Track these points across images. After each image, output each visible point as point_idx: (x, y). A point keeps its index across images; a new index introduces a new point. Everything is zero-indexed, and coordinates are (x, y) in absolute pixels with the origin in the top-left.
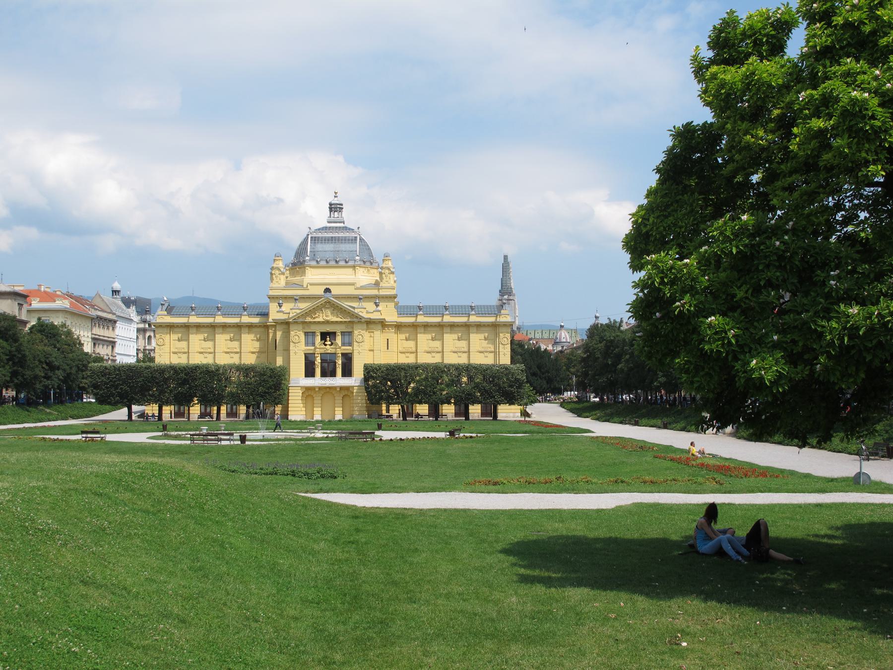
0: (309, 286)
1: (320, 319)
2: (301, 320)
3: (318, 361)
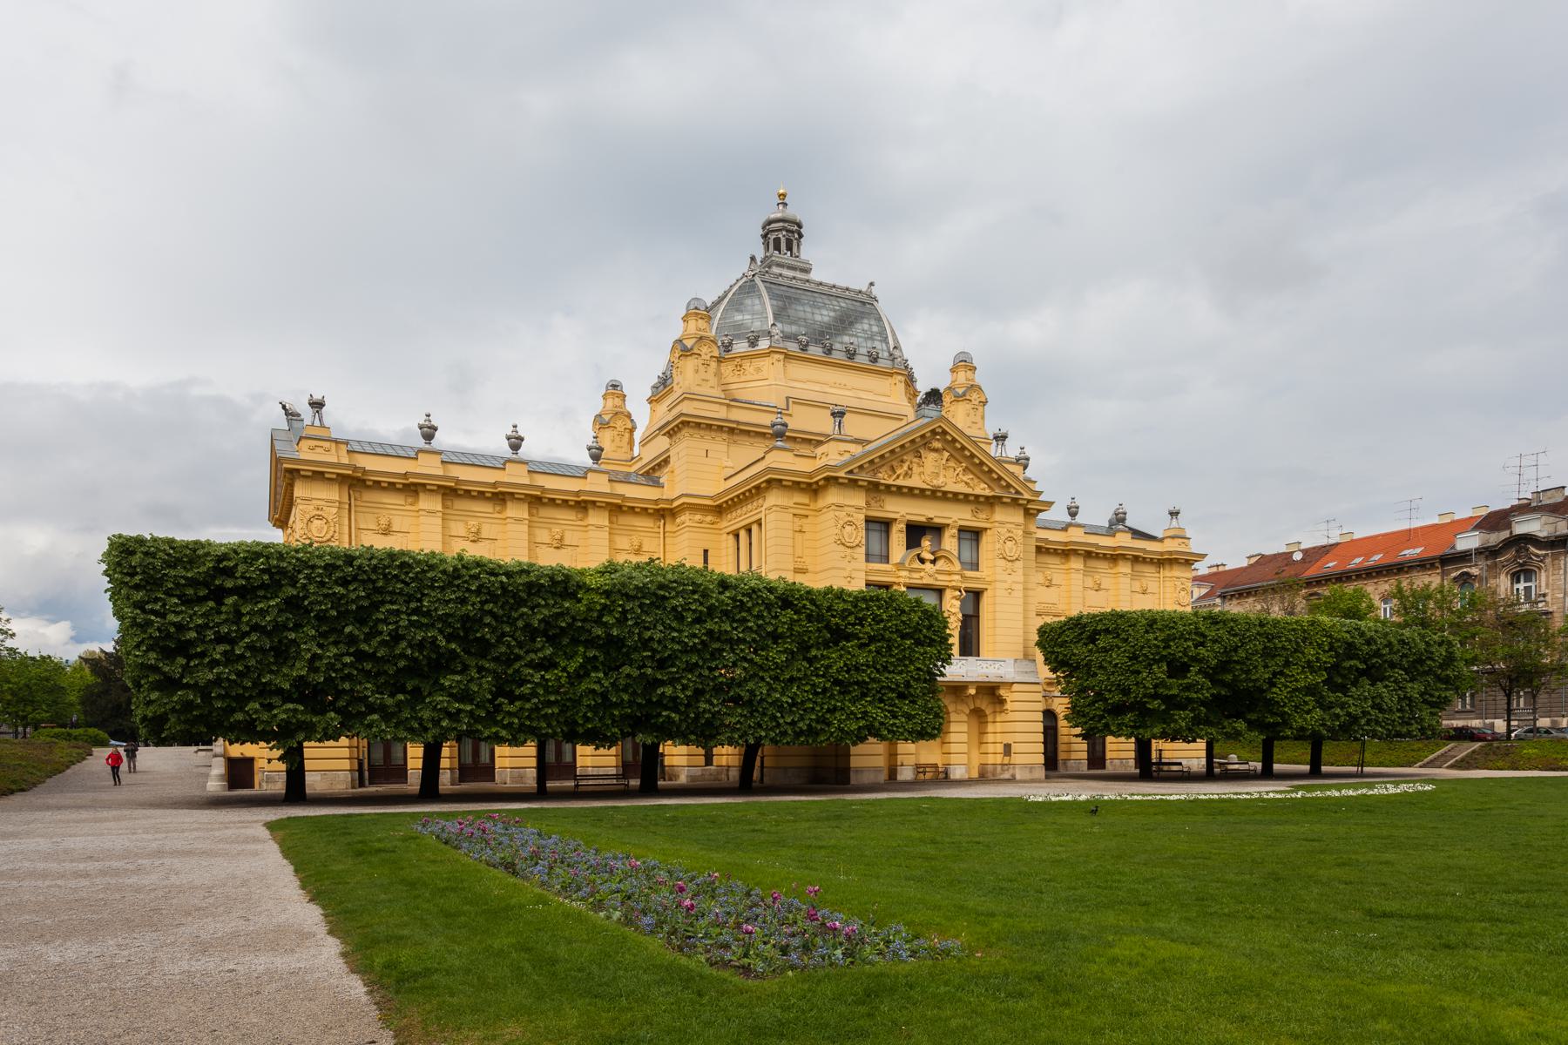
1: (915, 482)
2: (864, 477)
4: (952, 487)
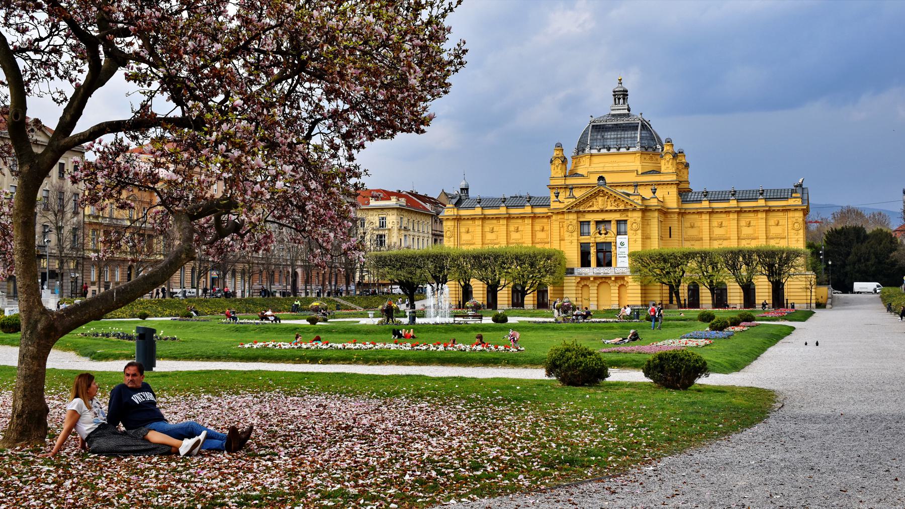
1: (595, 208)
2: (575, 209)
3: (593, 251)
4: (609, 208)
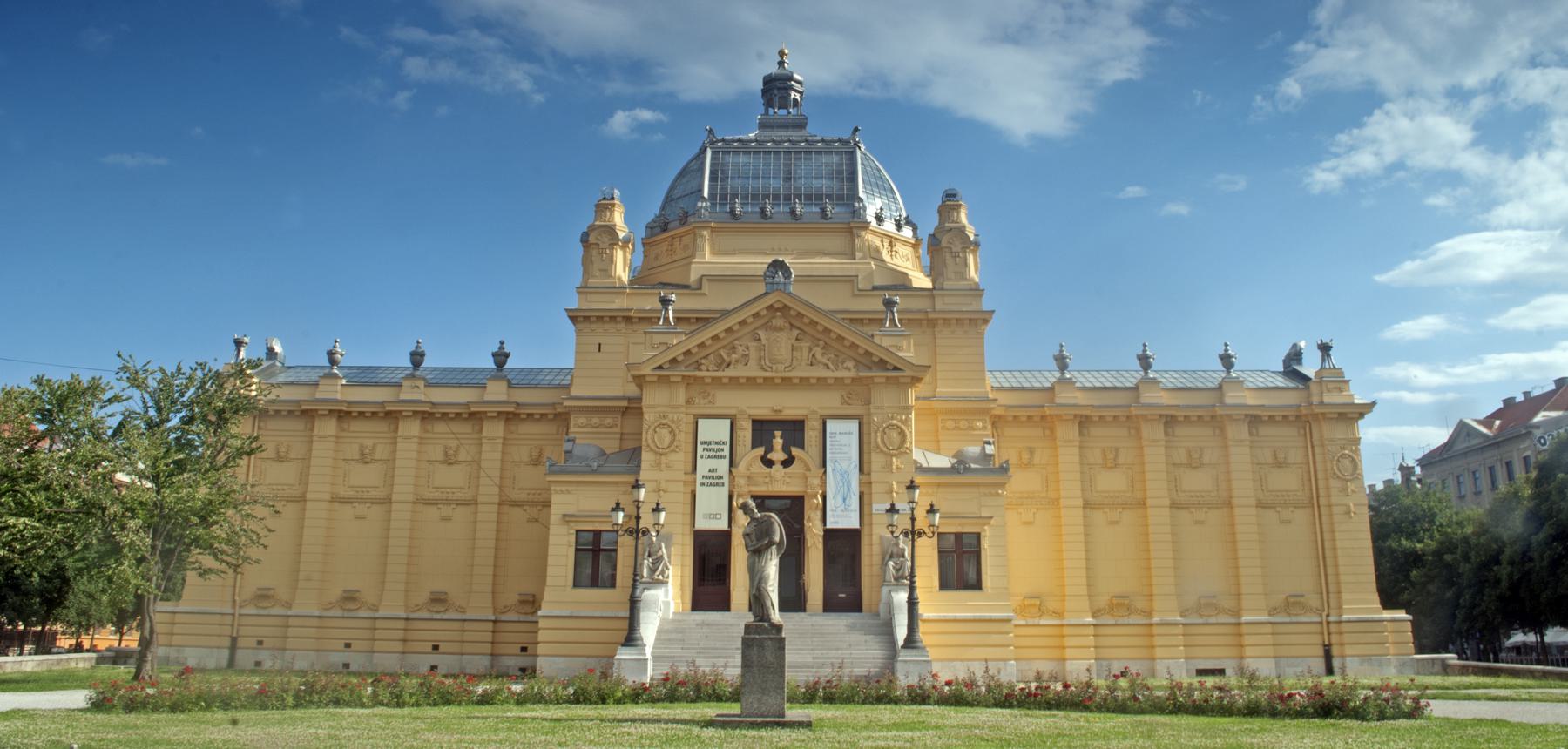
0: (706, 285)
1: (752, 371)
